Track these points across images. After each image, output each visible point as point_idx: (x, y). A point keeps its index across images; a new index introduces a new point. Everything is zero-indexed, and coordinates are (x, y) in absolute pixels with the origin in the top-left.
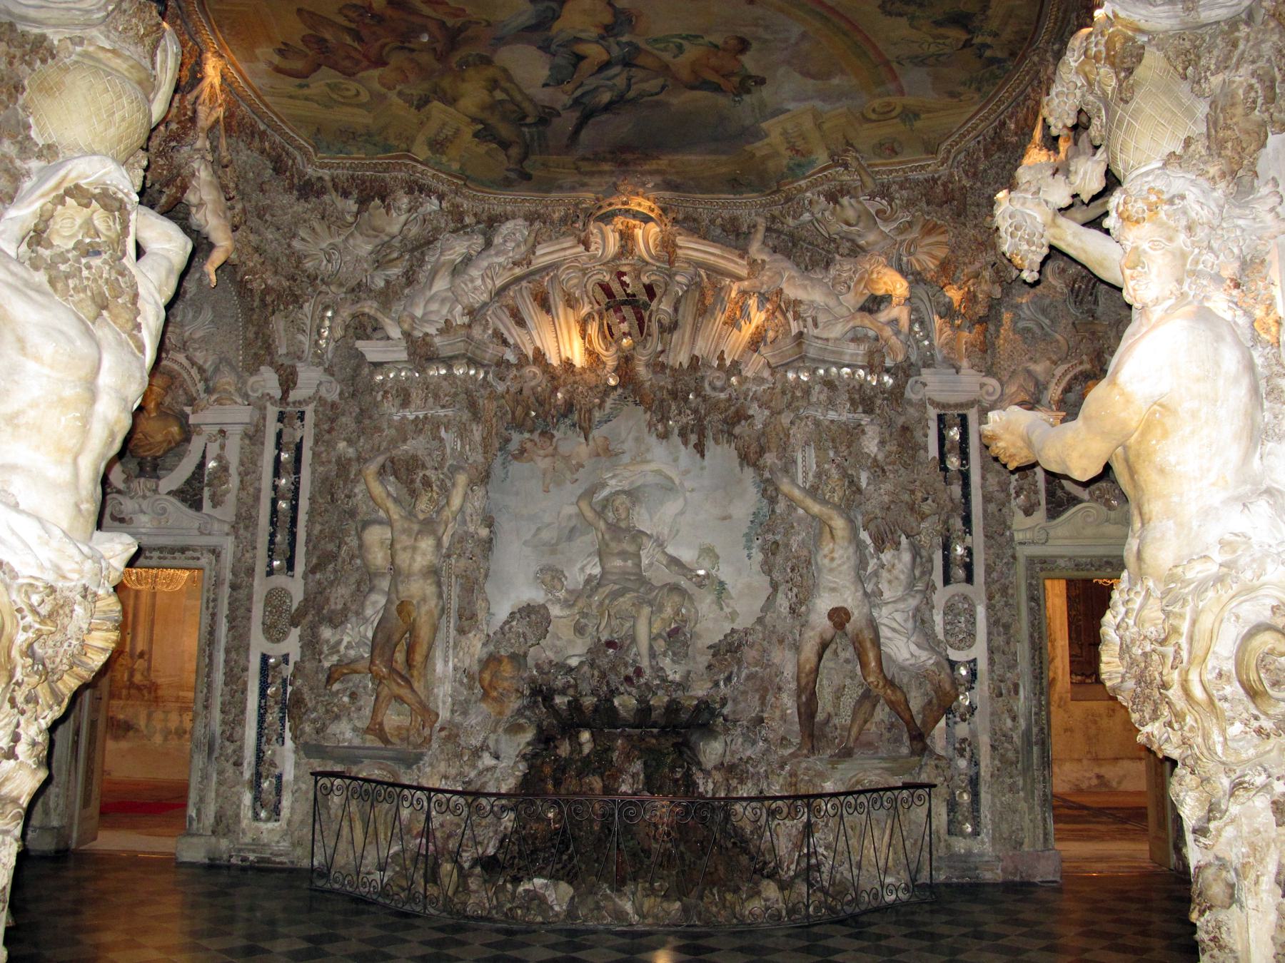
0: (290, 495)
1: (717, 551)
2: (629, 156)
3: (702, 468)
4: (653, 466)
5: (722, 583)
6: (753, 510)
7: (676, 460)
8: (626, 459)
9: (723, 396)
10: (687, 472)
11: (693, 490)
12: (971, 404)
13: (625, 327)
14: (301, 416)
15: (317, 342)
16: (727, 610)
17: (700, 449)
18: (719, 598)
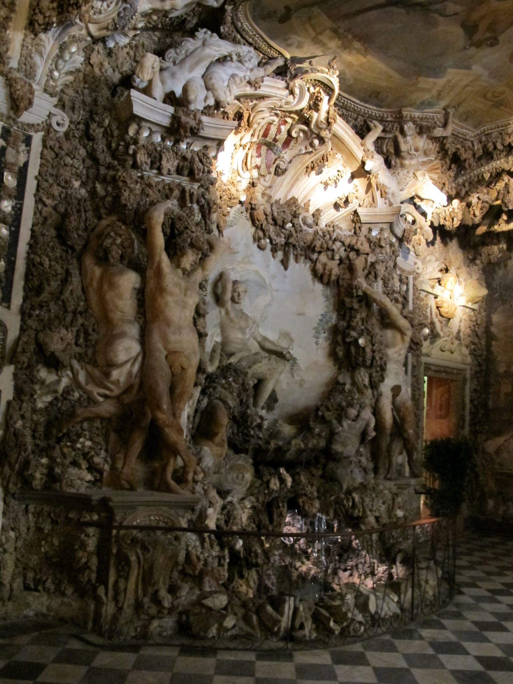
0: (10, 220)
1: (293, 336)
2: (357, 45)
3: (285, 277)
4: (253, 267)
5: (295, 359)
6: (322, 312)
7: (268, 266)
8: (239, 257)
9: (311, 231)
10: (274, 277)
11: (277, 291)
12: (410, 273)
13: (258, 161)
14: (28, 141)
15: (51, 72)
16: (297, 378)
17: (285, 263)
18: (292, 369)
